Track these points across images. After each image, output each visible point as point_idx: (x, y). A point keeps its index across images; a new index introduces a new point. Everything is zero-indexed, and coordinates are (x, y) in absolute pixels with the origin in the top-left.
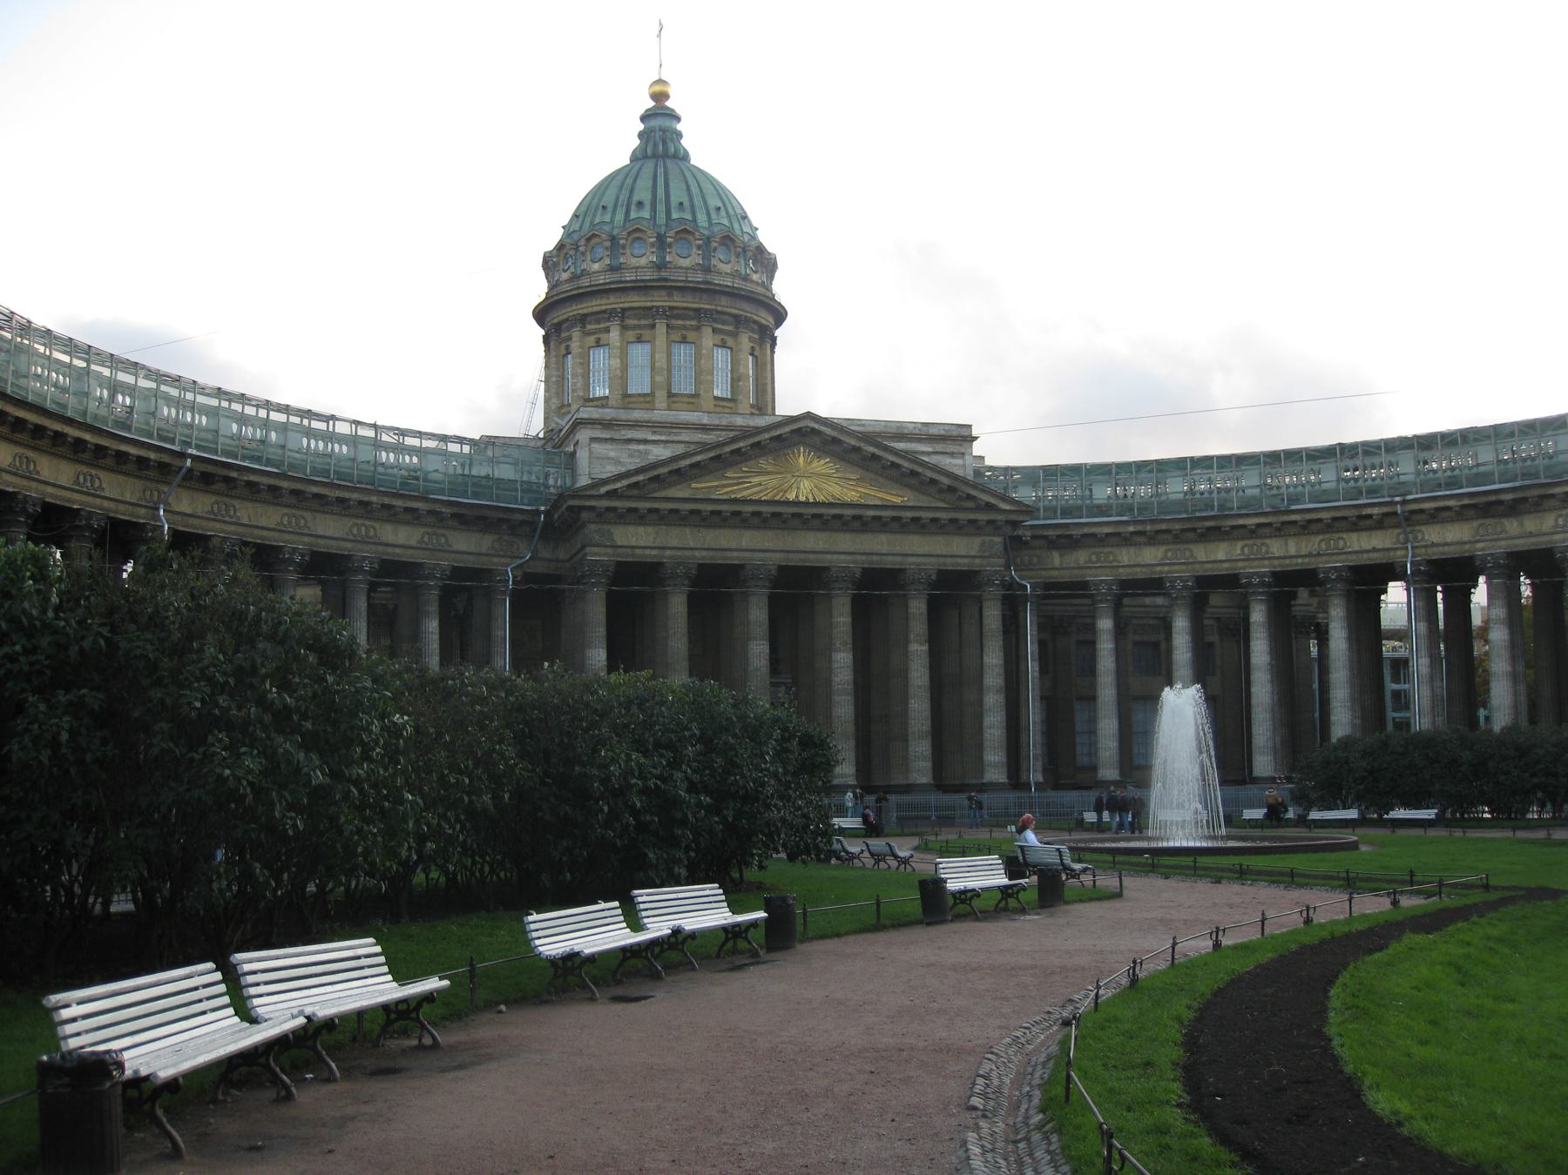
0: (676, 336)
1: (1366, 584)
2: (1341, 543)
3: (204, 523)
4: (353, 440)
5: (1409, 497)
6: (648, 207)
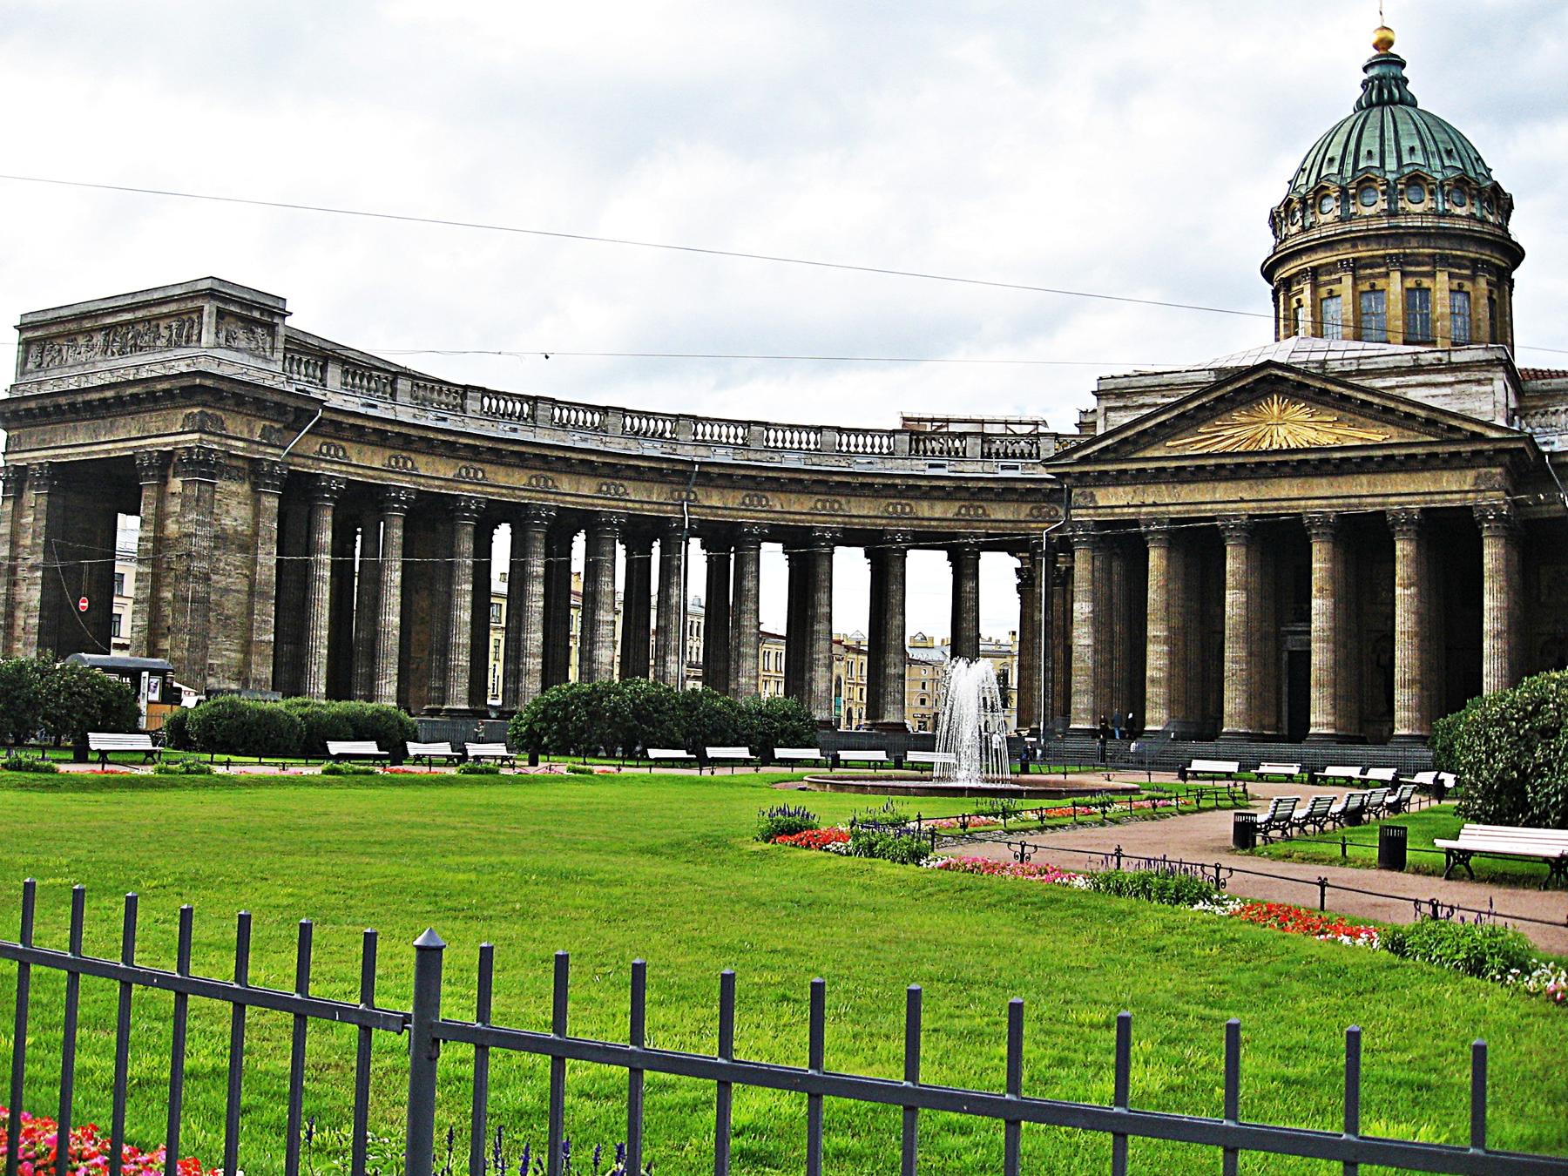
6: (1337, 163)
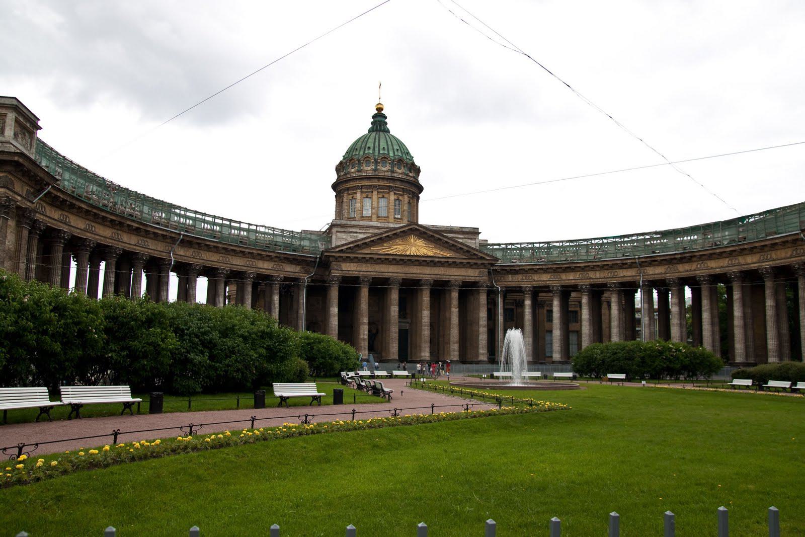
0: (381, 196)
1: (627, 290)
2: (616, 274)
3: (189, 259)
4: (248, 230)
5: (641, 256)
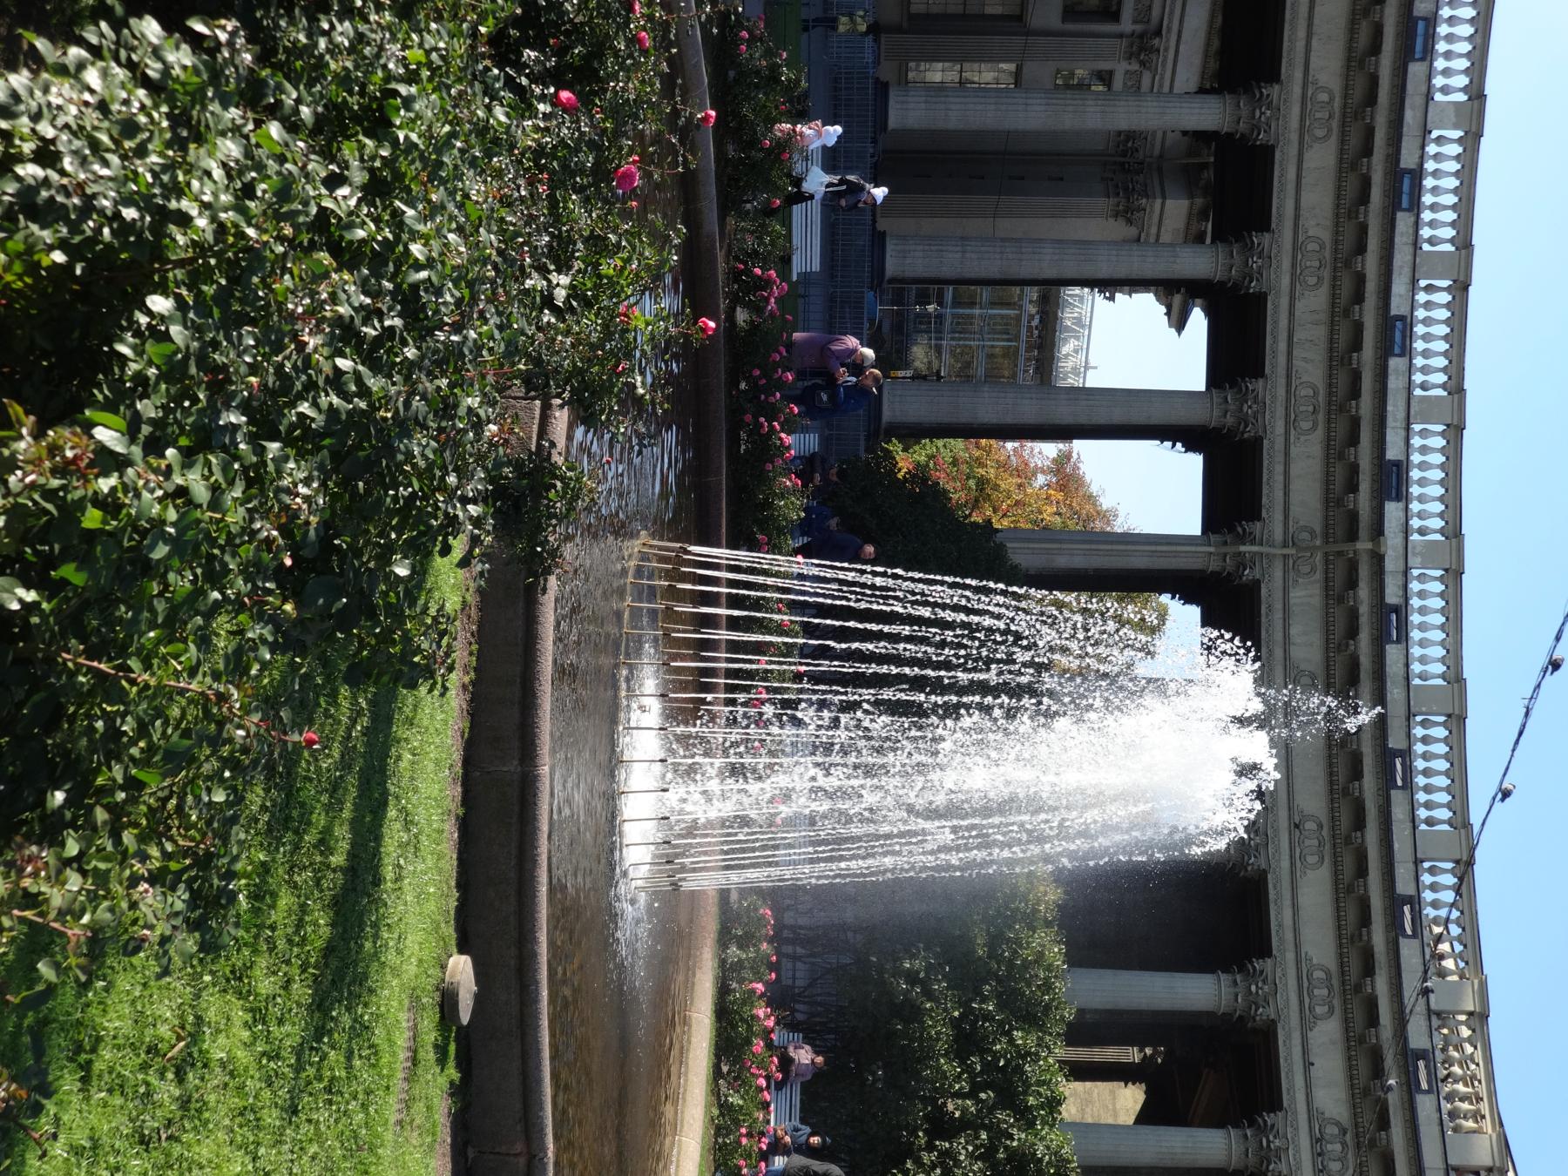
2: (1306, 425)
